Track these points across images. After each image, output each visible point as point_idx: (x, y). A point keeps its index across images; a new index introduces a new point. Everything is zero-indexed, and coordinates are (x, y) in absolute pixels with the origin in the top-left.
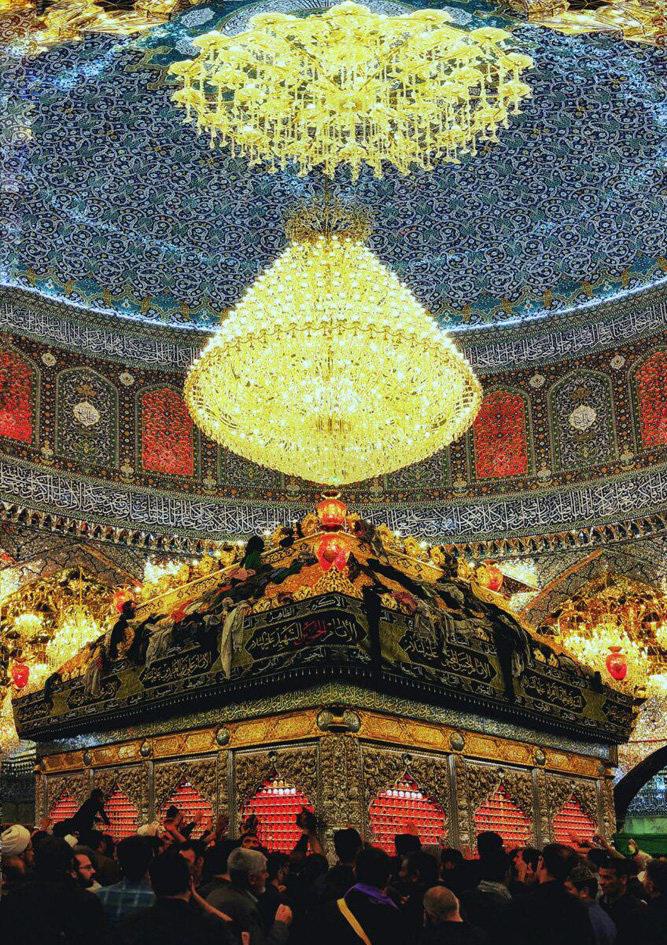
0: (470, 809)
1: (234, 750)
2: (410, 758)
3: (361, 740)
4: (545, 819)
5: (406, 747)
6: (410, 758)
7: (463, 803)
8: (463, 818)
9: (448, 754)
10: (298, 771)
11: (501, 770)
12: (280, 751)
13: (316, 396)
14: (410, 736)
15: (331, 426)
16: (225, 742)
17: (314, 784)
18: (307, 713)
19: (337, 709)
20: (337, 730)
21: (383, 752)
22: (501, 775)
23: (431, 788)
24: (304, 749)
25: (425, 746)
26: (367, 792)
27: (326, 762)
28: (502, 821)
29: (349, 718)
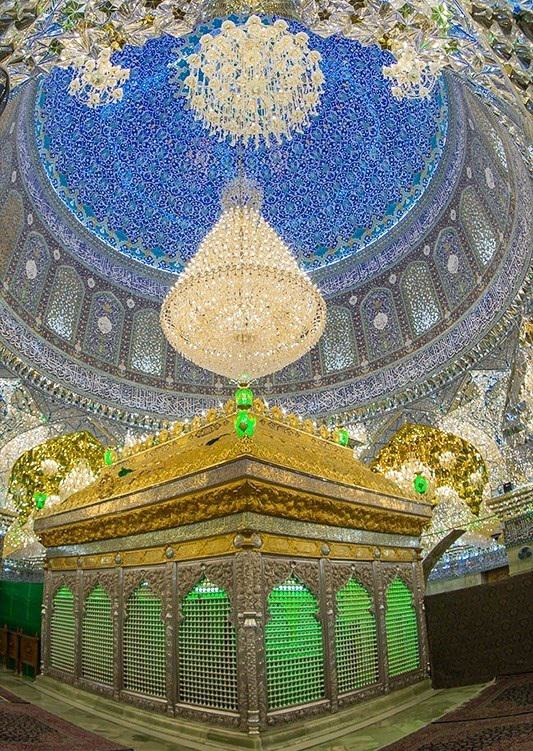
0: (333, 593)
1: (176, 562)
2: (295, 563)
3: (263, 553)
4: (381, 593)
5: (291, 556)
6: (295, 563)
7: (329, 589)
8: (329, 599)
9: (319, 559)
10: (220, 576)
11: (353, 565)
12: (208, 563)
13: (233, 320)
14: (295, 548)
15: (245, 338)
16: (172, 556)
17: (231, 584)
18: (227, 537)
19: (247, 533)
20: (246, 547)
21: (278, 560)
22: (353, 568)
23: (309, 582)
24: (224, 561)
25: (304, 555)
26: (267, 588)
27: (240, 570)
28: (351, 594)
29: (256, 539)
